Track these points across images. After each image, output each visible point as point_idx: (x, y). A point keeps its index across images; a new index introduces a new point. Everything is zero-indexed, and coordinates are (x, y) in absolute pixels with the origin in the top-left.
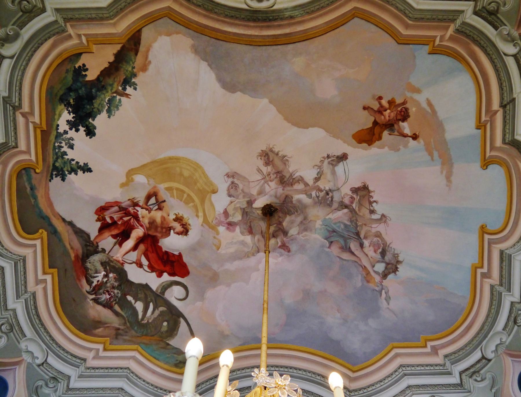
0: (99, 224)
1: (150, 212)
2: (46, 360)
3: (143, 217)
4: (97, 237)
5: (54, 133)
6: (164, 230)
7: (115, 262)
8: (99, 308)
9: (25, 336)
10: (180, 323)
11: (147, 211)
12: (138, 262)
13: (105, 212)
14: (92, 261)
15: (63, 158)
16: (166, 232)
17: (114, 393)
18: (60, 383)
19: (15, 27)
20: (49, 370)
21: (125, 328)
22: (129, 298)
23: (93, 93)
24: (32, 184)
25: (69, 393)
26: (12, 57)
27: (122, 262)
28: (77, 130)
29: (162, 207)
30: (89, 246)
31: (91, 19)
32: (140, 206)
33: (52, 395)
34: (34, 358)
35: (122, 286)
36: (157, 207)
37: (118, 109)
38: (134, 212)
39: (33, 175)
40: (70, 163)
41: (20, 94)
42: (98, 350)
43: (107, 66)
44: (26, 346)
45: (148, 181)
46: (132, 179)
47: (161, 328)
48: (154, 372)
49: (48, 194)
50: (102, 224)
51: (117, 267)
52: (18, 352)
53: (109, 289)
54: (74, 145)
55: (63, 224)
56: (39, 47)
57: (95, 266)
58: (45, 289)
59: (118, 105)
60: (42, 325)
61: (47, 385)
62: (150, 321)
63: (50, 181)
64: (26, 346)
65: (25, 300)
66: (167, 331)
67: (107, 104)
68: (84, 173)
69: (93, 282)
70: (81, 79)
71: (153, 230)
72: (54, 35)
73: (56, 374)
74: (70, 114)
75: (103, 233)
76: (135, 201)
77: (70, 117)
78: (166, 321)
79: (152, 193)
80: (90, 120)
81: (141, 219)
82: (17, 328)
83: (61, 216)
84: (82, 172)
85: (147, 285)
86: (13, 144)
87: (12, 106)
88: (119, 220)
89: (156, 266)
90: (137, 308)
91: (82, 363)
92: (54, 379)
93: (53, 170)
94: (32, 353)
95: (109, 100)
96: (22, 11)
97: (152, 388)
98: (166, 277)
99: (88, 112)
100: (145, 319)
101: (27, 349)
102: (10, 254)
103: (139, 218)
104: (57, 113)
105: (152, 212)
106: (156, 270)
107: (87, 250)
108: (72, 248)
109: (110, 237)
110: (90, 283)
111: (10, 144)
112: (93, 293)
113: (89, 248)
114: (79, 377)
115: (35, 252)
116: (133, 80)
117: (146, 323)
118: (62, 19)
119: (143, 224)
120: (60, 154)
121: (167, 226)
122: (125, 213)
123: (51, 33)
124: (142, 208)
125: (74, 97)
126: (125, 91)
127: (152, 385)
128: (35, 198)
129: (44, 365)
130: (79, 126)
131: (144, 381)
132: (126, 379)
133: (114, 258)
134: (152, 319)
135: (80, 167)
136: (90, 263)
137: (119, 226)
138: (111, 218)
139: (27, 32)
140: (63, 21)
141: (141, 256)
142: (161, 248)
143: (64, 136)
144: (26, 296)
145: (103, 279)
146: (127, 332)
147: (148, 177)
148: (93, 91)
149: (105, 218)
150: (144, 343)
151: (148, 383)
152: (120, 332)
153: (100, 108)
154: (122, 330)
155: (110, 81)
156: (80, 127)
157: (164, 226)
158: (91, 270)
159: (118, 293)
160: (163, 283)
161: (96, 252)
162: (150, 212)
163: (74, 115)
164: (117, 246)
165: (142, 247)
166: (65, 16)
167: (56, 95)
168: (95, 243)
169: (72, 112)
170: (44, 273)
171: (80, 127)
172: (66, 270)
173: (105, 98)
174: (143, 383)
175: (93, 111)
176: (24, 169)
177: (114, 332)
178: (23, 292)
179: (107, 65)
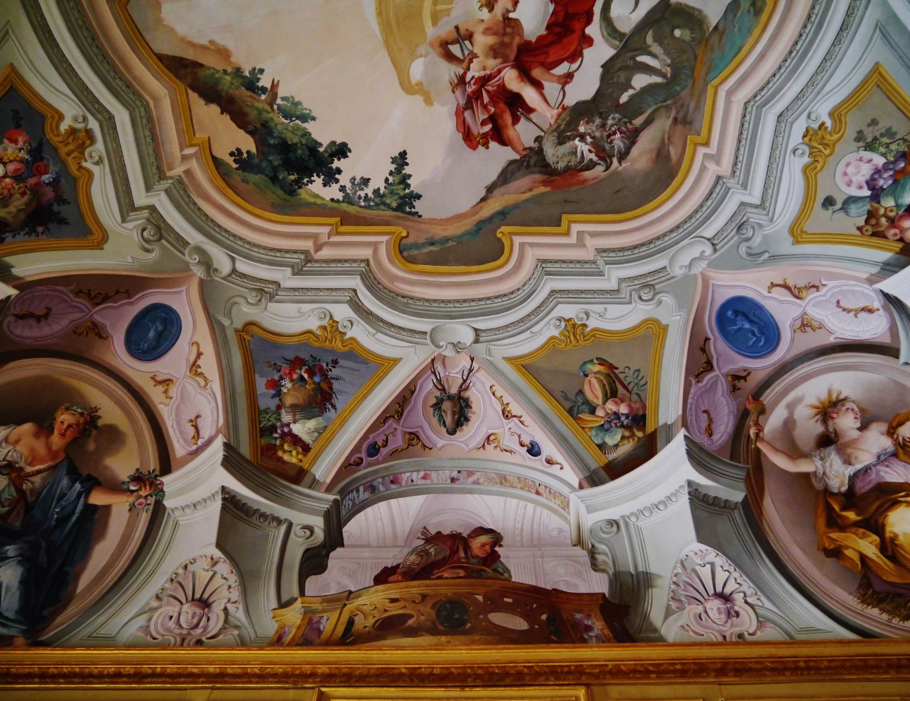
0: (493, 145)
1: (476, 56)
2: (709, 240)
3: (484, 69)
4: (514, 149)
5: (345, 206)
6: (509, 30)
7: (558, 121)
8: (635, 151)
9: (665, 267)
10: (680, 4)
11: (474, 60)
12: (563, 81)
13: (472, 133)
14: (555, 160)
15: (384, 196)
16: (512, 27)
17: (784, 131)
18: (749, 219)
19: (186, 252)
20: (725, 235)
21: (676, 107)
22: (624, 98)
23: (276, 142)
24: (424, 243)
25: (767, 205)
26: (233, 260)
27: (560, 110)
28: (339, 171)
29: (467, 33)
30: (528, 162)
31: (154, 137)
32: (465, 73)
33: (765, 232)
34: (702, 257)
35: (601, 110)
36: (467, 43)
37: (299, 103)
38: (474, 84)
39: (409, 240)
40: (391, 184)
41: (287, 251)
42: (705, 155)
43: (228, 117)
44: (681, 267)
45: (421, 56)
46: (417, 84)
47: (684, 41)
48: (762, 57)
49: (442, 220)
50: (493, 139)
51: (568, 118)
52: (688, 279)
53: (605, 134)
54: (362, 178)
55: (490, 201)
56: (212, 221)
57: (564, 155)
58: (593, 235)
59: (292, 103)
60: (650, 242)
61: (748, 240)
62: (669, 61)
63: (420, 216)
64: (681, 267)
65: (607, 264)
66: (692, 30)
67: (292, 121)
68: (407, 164)
69: (591, 160)
70: (256, 161)
71: (508, 51)
72: (189, 196)
73: (734, 225)
74: (314, 181)
75: (508, 138)
76: (456, 81)
77: (318, 181)
78: (673, 31)
79: (443, 51)
80: (321, 150)
81: (488, 72)
82: (649, 279)
83: (478, 204)
84: (405, 167)
85: (604, 66)
86: (363, 265)
87: (306, 264)
88: (488, 111)
89: (572, 48)
90: (644, 85)
91: (724, 183)
92: (740, 227)
93: (404, 212)
94: (694, 260)
95: (286, 117)
96: (159, 240)
97: (789, 61)
98: (593, 30)
99: (308, 153)
100: (664, 71)
101: (685, 266)
102: (532, 280)
103: (485, 76)
104: (312, 200)
105: (475, 51)
106: (579, 48)
107: (535, 165)
108: (530, 190)
109: (517, 127)
110: (591, 165)
111: (363, 269)
112: (609, 161)
113: (532, 163)
114: (746, 189)
115: (532, 245)
116: (247, 74)
117: (672, 70)
118: (162, 182)
119: (495, 69)
120: (377, 200)
121: (502, 25)
122: (477, 100)
123: (186, 199)
124: (468, 69)
125: (286, 173)
126: (267, 89)
127: (785, 60)
128: (447, 240)
129: (715, 242)
130: (331, 168)
131: (774, 75)
132: (764, 109)
133: (552, 122)
134: (665, 58)
135: (399, 170)
136: (558, 163)
137: (499, 111)
138: (484, 123)
139: (193, 236)
140: (165, 182)
141: (553, 75)
142: (540, 38)
143: (348, 191)
144: (600, 262)
145: (586, 144)
146: (682, 105)
147: (413, 57)
148: (272, 142)
149: (483, 134)
150: (707, 74)
151: (780, 68)
152: (680, 117)
153: (299, 133)
154: (678, 112)
155: (253, 114)
156: (334, 166)
157: (501, 31)
158: (570, 162)
159: (614, 118)
160: (603, 36)
161: (540, 151)
162: (476, 56)
163: (315, 175)
164: (532, 116)
165: (537, 73)
166: (156, 178)
167: (285, 200)
168: (525, 153)
169: (310, 178)
170: (567, 233)
171: (334, 166)
172: (566, 201)
173: (283, 123)
174: (777, 77)
175: (306, 145)
176: (401, 252)
177: (679, 127)
178: (594, 266)
179: (227, 117)
